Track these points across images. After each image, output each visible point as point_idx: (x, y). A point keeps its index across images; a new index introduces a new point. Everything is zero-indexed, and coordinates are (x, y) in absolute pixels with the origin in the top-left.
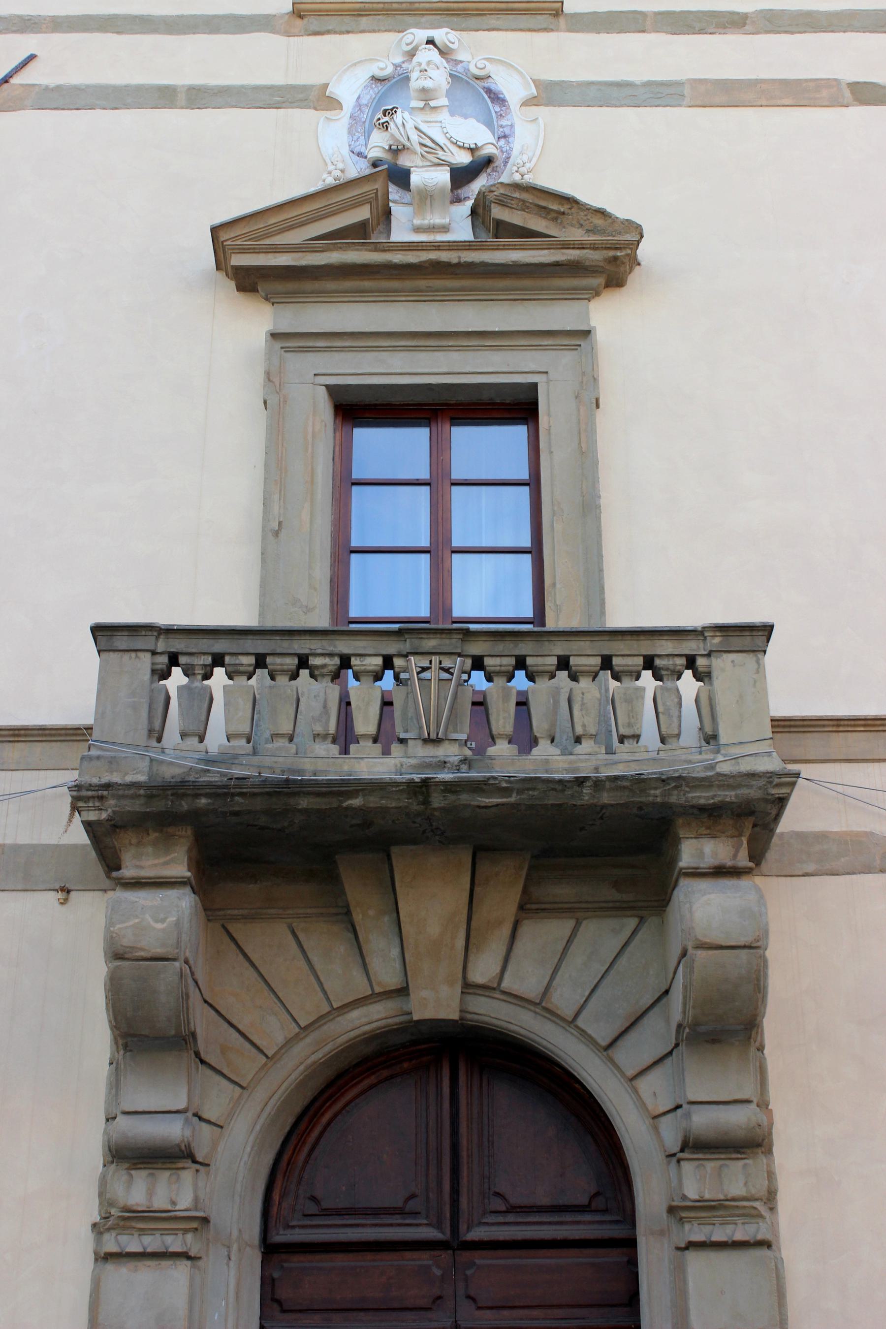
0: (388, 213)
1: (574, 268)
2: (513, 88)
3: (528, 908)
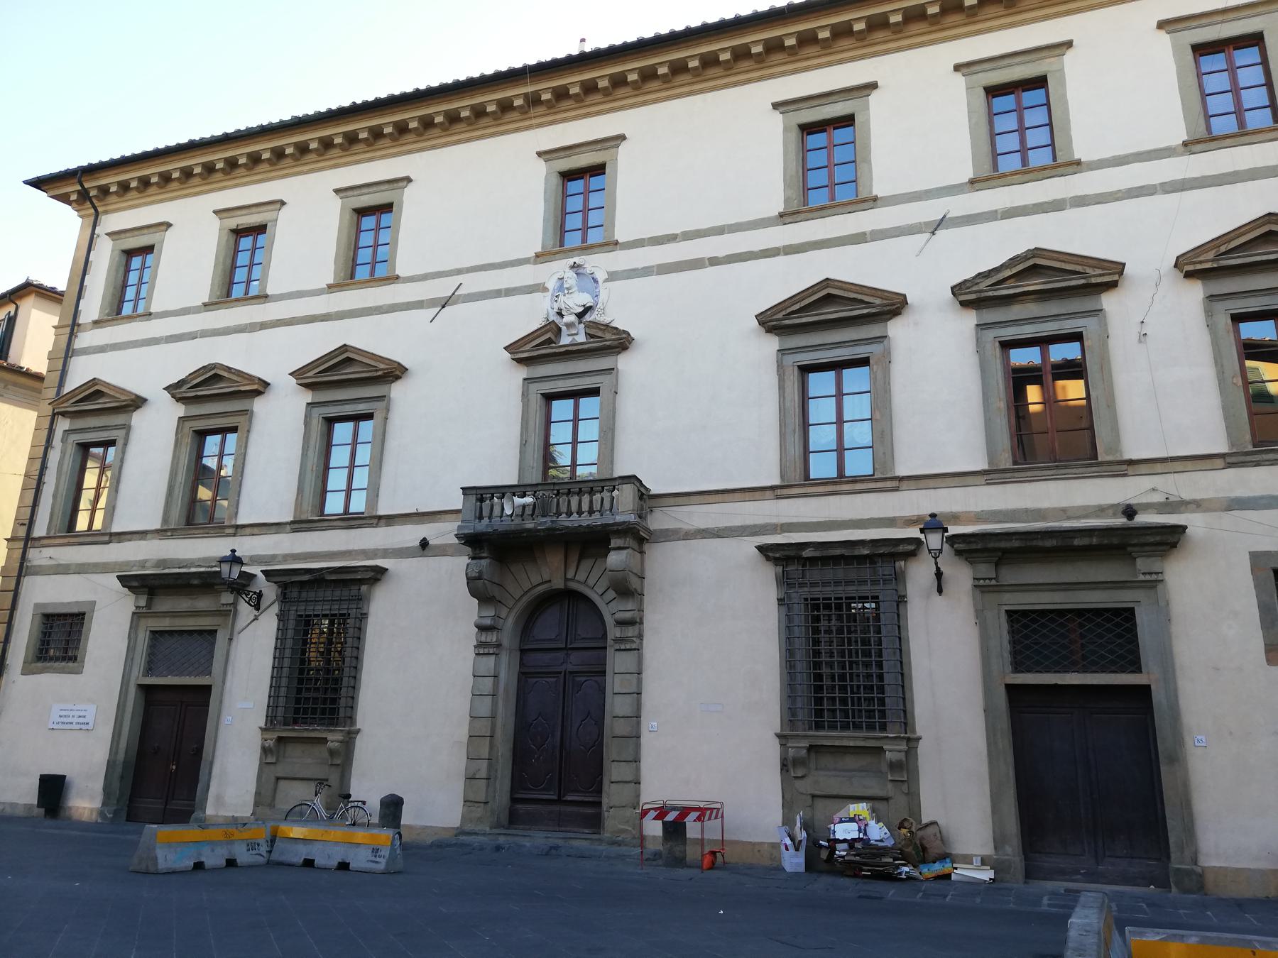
0: (560, 329)
1: (609, 347)
2: (601, 276)
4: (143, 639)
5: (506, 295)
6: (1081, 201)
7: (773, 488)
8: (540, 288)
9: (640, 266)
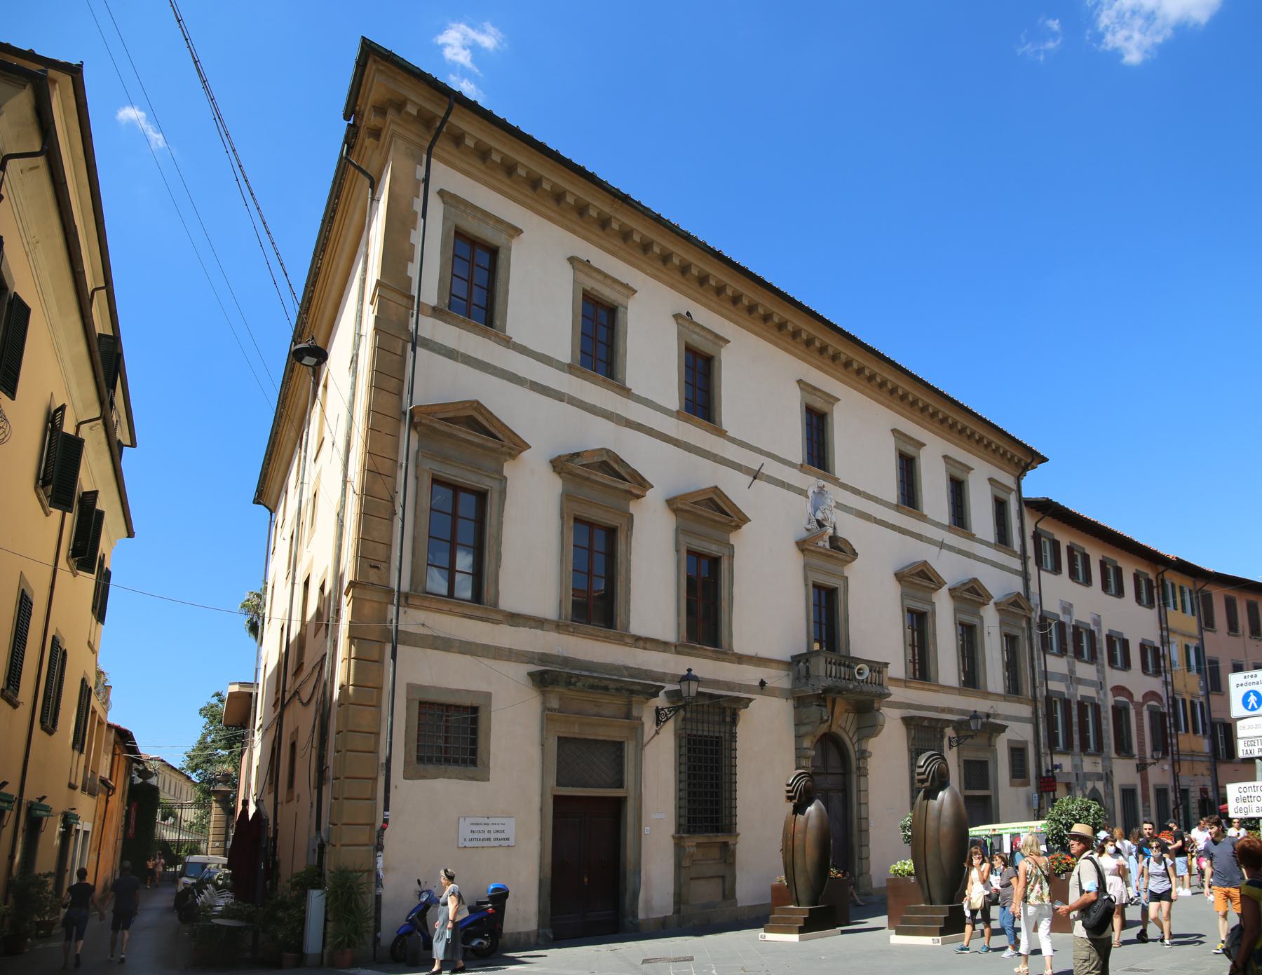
4: (553, 745)
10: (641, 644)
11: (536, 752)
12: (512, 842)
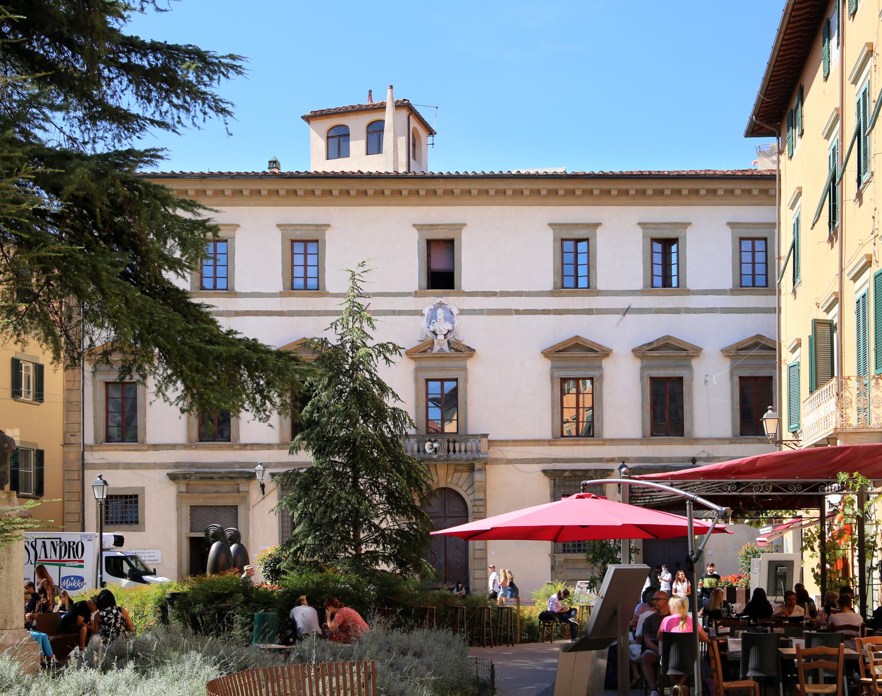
2: (455, 311)
3: (455, 471)
4: (186, 511)
5: (399, 315)
6: (688, 311)
7: (549, 441)
8: (419, 313)
9: (477, 308)
10: (249, 447)
11: (173, 515)
12: (159, 562)
